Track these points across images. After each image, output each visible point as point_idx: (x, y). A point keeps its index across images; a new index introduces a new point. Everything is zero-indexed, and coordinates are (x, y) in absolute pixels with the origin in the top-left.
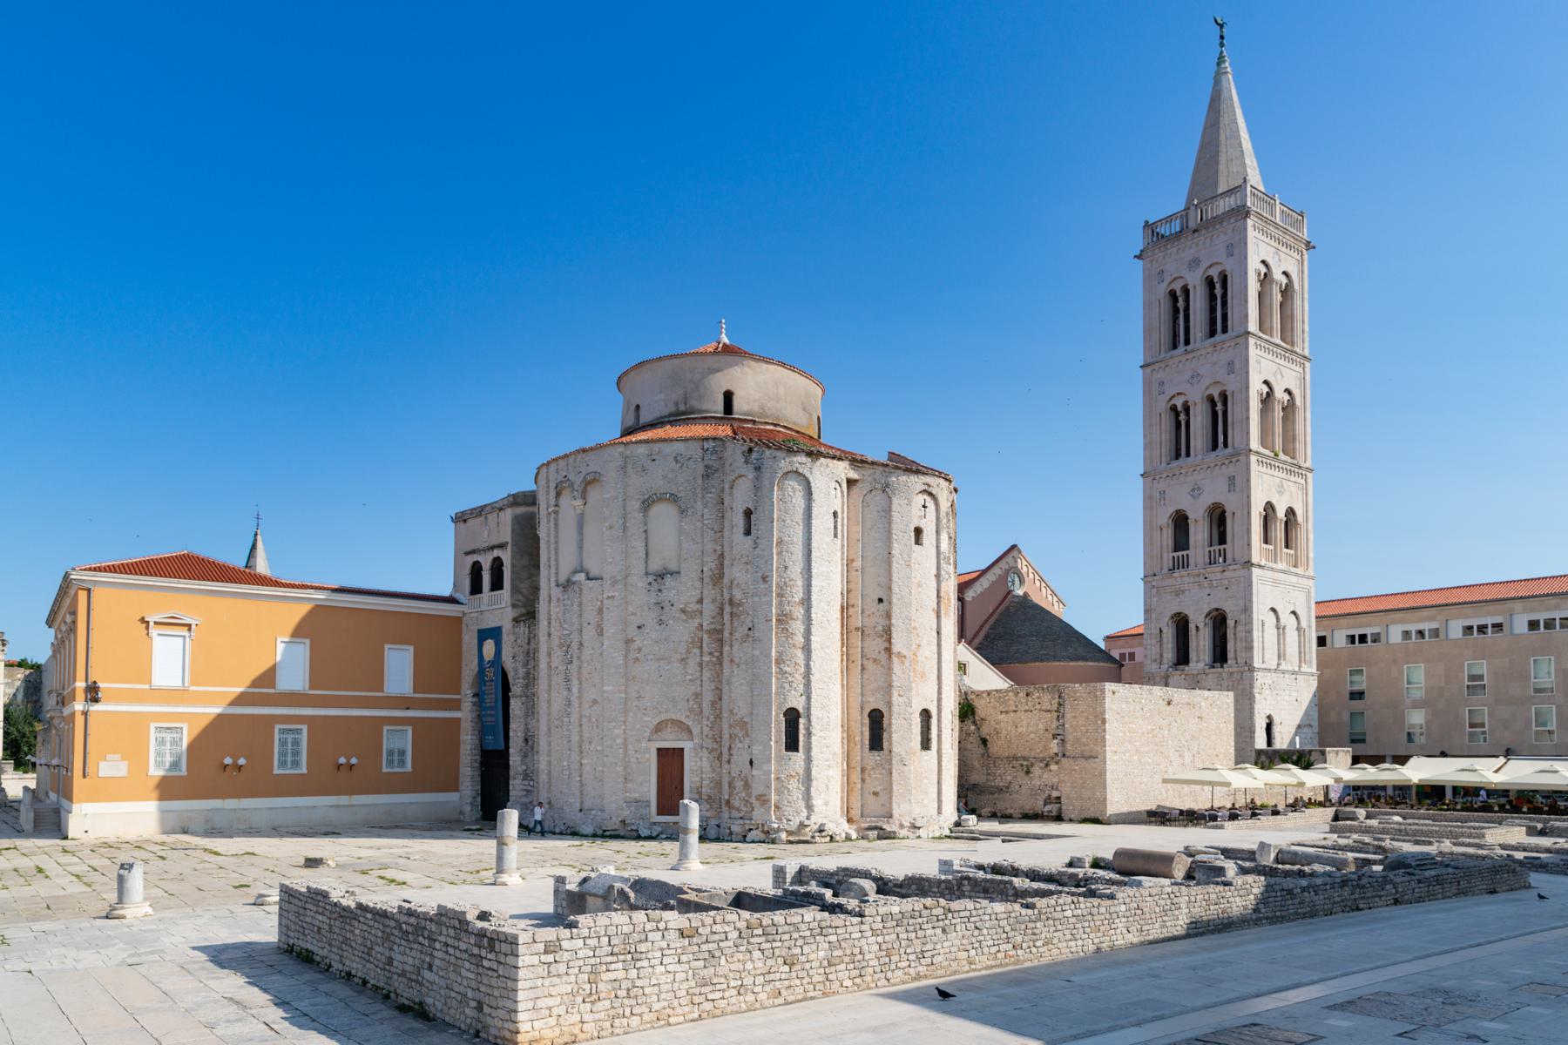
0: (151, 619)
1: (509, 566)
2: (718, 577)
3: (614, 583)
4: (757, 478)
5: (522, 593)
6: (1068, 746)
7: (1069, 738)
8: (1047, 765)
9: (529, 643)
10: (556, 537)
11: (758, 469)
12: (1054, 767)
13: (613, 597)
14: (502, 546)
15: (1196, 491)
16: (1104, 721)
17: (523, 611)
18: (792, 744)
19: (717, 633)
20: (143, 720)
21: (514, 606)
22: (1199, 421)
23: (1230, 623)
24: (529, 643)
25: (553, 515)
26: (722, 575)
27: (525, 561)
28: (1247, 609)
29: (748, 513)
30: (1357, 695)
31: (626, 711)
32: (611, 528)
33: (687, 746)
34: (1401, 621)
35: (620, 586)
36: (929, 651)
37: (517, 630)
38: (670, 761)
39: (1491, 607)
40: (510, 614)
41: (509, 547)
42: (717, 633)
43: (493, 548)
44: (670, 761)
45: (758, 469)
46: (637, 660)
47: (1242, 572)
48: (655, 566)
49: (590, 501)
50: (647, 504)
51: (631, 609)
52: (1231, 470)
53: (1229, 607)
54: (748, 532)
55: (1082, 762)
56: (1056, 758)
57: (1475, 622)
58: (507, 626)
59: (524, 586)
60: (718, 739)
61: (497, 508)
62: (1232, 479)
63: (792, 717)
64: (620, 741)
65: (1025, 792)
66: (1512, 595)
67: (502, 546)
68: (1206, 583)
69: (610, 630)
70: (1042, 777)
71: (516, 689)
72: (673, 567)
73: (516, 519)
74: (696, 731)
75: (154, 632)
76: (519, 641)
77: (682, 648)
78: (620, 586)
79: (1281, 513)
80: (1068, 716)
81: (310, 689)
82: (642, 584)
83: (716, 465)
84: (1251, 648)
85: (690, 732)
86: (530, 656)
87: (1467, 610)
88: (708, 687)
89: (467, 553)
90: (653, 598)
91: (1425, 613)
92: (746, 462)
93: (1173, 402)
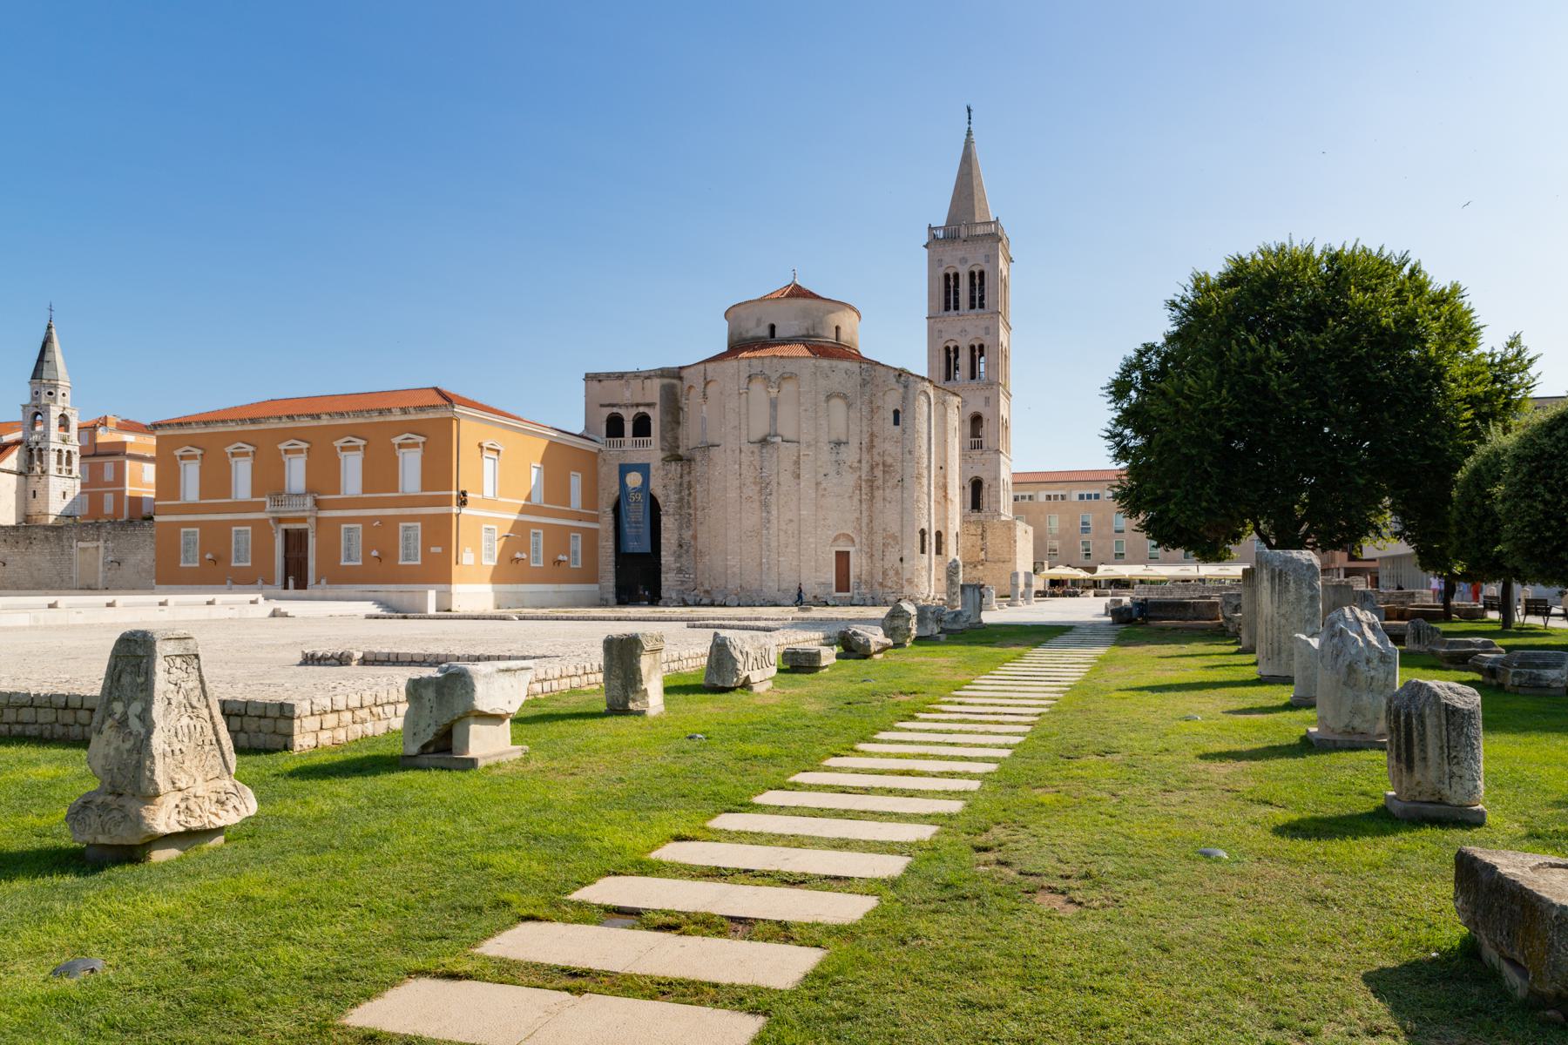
0: (485, 445)
1: (658, 422)
2: (871, 447)
3: (809, 446)
4: (906, 393)
5: (667, 441)
6: (989, 556)
7: (990, 551)
8: (975, 566)
9: (681, 477)
10: (748, 410)
11: (906, 387)
12: (980, 567)
13: (808, 455)
14: (649, 405)
16: (1015, 541)
17: (668, 453)
19: (871, 482)
20: (479, 521)
21: (662, 450)
22: (964, 360)
23: (985, 486)
24: (681, 477)
25: (744, 395)
26: (872, 447)
27: (669, 418)
28: (997, 478)
29: (896, 413)
31: (816, 528)
32: (806, 410)
33: (851, 549)
34: (1046, 489)
35: (813, 448)
37: (668, 467)
38: (843, 558)
39: (1095, 484)
40: (660, 455)
41: (658, 407)
43: (638, 405)
44: (843, 558)
45: (906, 387)
46: (823, 495)
47: (994, 456)
48: (834, 438)
49: (784, 391)
50: (829, 397)
51: (819, 463)
52: (987, 393)
53: (984, 476)
54: (896, 422)
55: (1001, 565)
56: (982, 563)
57: (1085, 493)
59: (669, 436)
60: (871, 546)
61: (648, 376)
62: (987, 399)
64: (813, 546)
66: (1073, 479)
67: (649, 405)
68: (970, 460)
69: (806, 475)
72: (843, 439)
73: (663, 387)
74: (857, 540)
75: (486, 454)
76: (670, 476)
77: (850, 490)
78: (813, 448)
80: (989, 538)
81: (545, 502)
82: (826, 448)
83: (867, 378)
84: (999, 502)
85: (853, 542)
87: (1082, 485)
88: (865, 514)
89: (602, 406)
90: (834, 457)
91: (1060, 485)
92: (897, 382)
93: (948, 344)
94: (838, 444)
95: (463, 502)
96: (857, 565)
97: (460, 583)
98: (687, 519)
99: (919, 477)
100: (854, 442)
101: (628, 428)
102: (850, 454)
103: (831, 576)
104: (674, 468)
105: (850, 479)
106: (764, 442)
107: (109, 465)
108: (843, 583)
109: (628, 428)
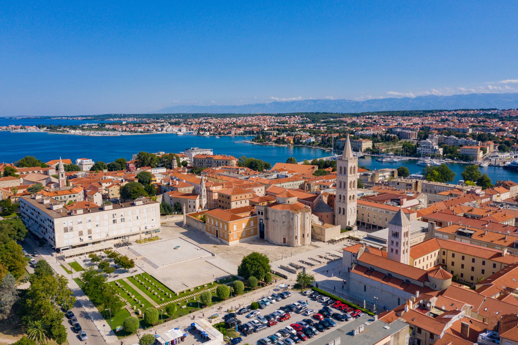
2: (289, 223)
15: (342, 193)
18: (296, 239)
19: (289, 228)
20: (233, 234)
30: (363, 215)
36: (308, 228)
38: (284, 239)
42: (289, 228)
44: (284, 239)
58: (264, 219)
63: (296, 236)
65: (318, 238)
70: (319, 236)
71: (265, 226)
79: (352, 196)
86: (267, 223)
94: (284, 222)
95: (230, 232)
96: (287, 240)
97: (232, 241)
98: (267, 228)
99: (295, 228)
100: (286, 222)
101: (261, 213)
102: (286, 224)
103: (282, 241)
104: (266, 220)
105: (286, 227)
106: (274, 221)
107: (211, 193)
108: (284, 242)
109: (261, 213)
